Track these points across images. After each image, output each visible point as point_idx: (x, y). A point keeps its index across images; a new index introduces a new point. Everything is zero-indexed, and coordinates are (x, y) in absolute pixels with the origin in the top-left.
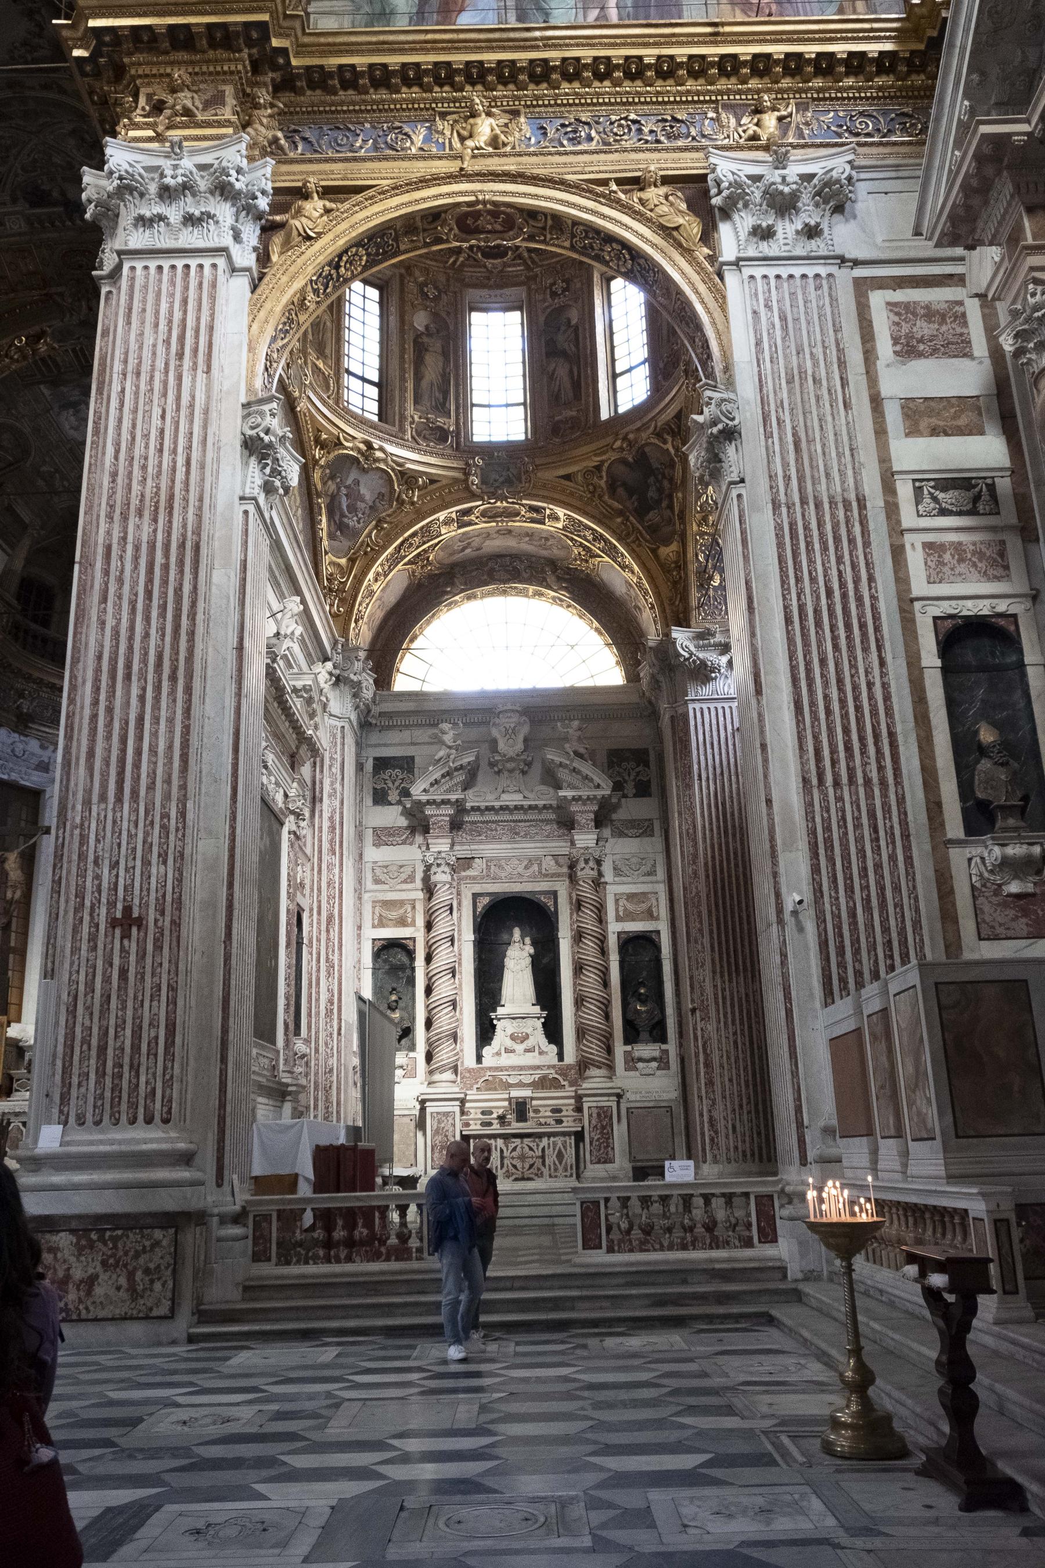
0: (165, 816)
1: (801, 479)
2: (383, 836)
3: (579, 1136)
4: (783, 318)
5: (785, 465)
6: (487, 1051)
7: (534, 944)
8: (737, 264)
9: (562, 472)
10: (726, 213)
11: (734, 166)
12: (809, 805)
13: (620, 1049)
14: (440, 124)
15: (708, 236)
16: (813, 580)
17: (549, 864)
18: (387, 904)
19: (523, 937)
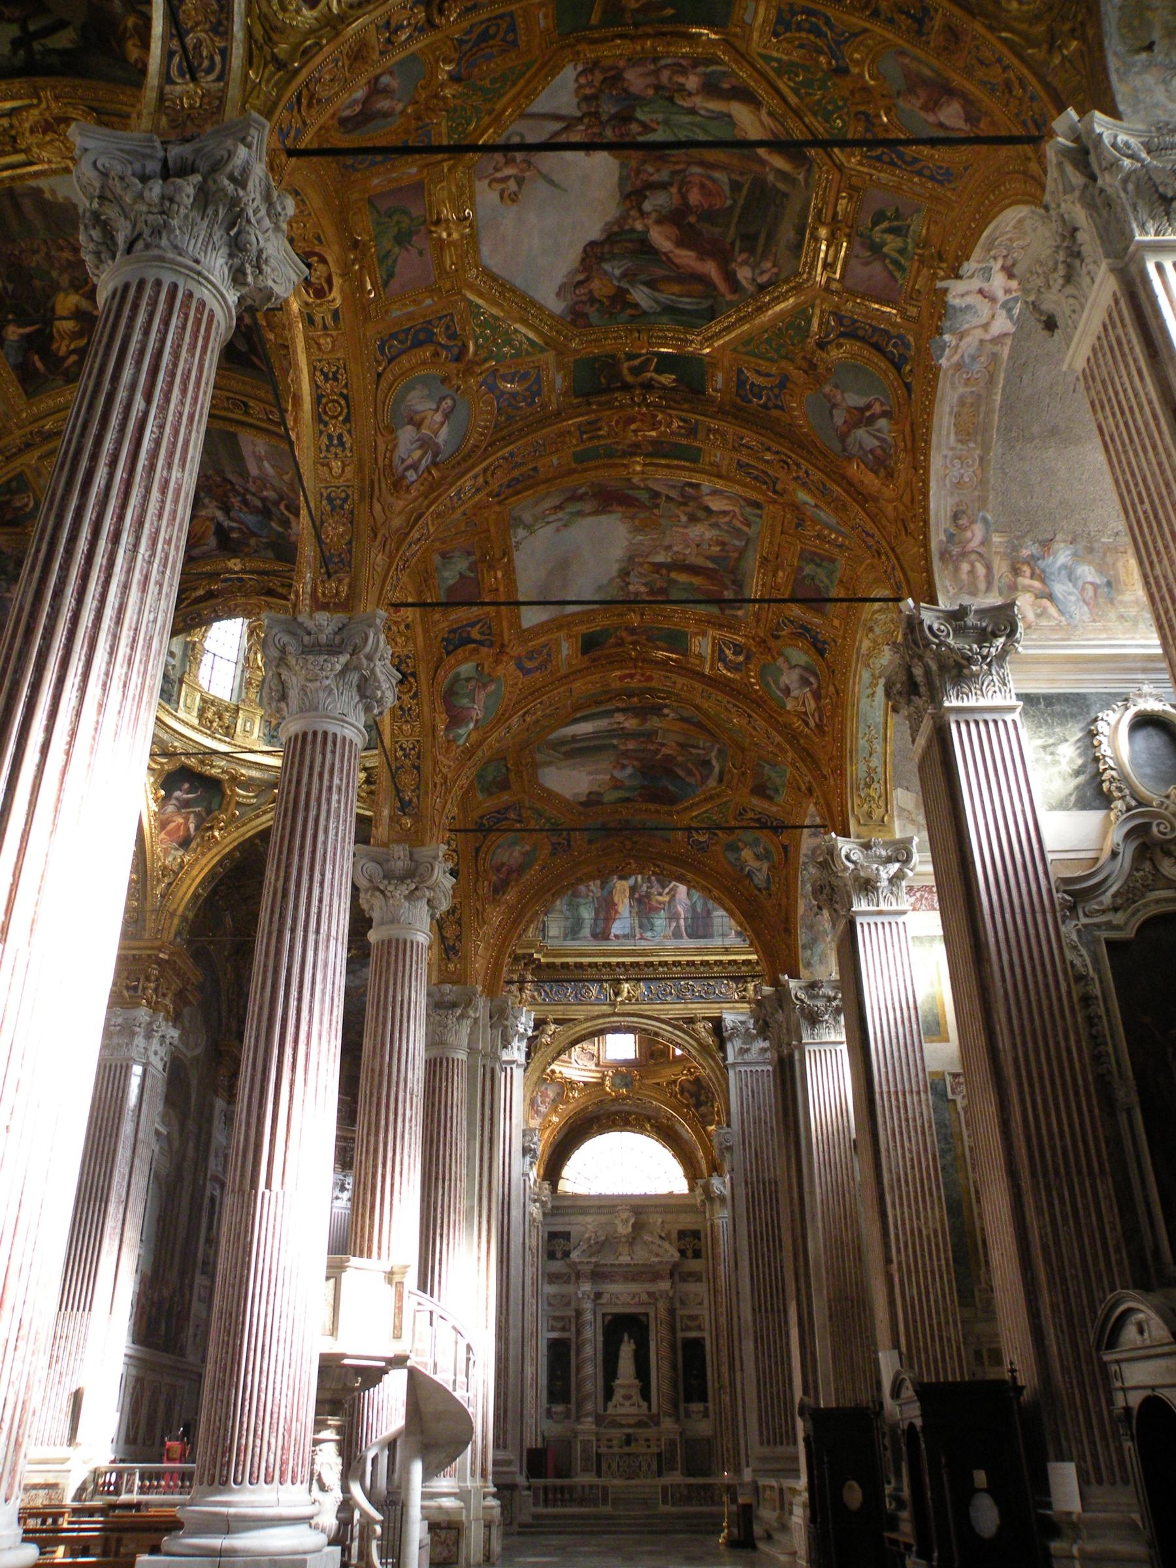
2: (553, 1278)
6: (610, 1404)
8: (734, 1065)
10: (730, 1038)
11: (732, 1017)
12: (755, 1321)
13: (682, 1406)
14: (606, 985)
15: (722, 1048)
17: (644, 1297)
18: (555, 1318)
19: (630, 1337)
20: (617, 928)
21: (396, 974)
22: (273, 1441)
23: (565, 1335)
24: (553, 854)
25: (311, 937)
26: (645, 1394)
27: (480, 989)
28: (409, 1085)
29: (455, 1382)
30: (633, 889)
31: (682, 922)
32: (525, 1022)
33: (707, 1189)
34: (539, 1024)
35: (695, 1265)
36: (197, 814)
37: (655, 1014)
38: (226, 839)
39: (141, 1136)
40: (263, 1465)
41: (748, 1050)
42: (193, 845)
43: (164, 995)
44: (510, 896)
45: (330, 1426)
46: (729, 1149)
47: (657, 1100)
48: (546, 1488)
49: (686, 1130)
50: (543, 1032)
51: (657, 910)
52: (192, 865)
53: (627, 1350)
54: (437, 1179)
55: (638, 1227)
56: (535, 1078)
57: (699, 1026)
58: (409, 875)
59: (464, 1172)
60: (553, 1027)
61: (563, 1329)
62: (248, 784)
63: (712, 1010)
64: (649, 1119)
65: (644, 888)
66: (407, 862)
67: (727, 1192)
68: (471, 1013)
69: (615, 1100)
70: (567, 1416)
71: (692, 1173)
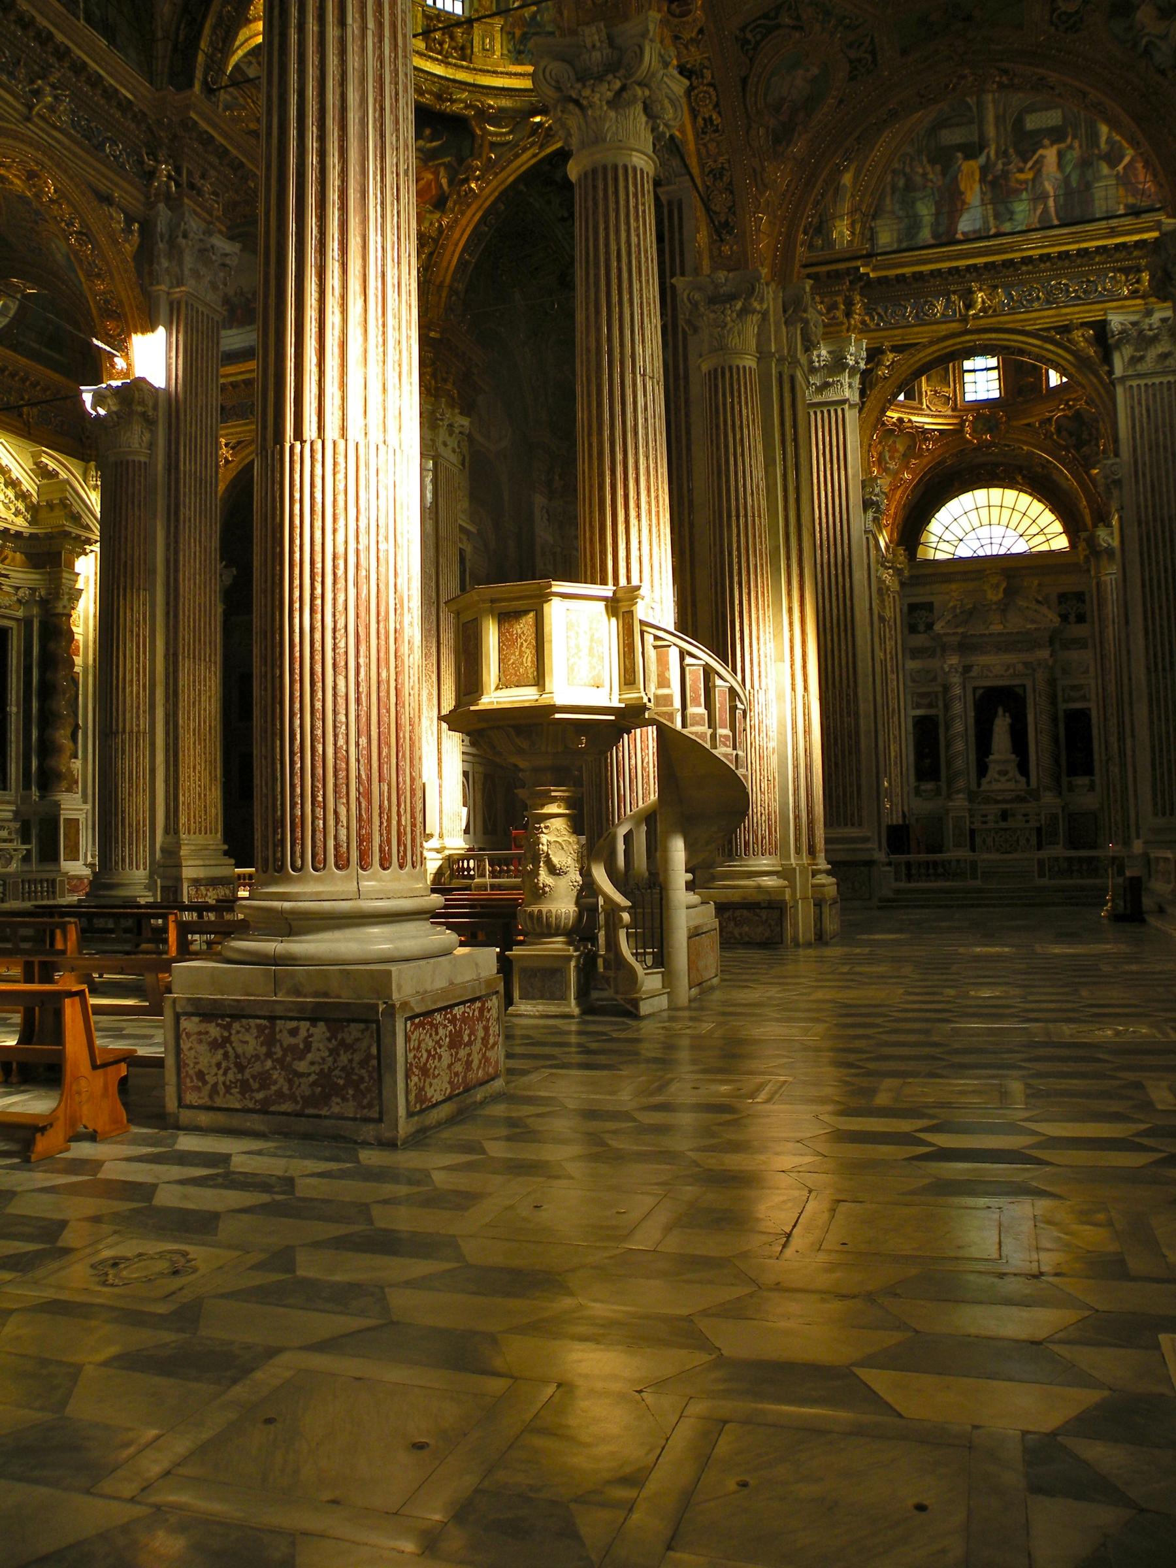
0: (848, 695)
1: (1154, 506)
2: (915, 653)
3: (1039, 830)
4: (1148, 411)
5: (1146, 500)
6: (984, 781)
7: (1011, 717)
8: (1123, 379)
9: (1026, 422)
10: (1117, 346)
11: (1120, 318)
12: (1149, 681)
13: (1065, 780)
14: (954, 298)
15: (1107, 359)
16: (1158, 563)
17: (1020, 667)
18: (922, 695)
19: (1004, 712)
20: (965, 225)
21: (606, 215)
22: (342, 810)
23: (932, 712)
24: (852, 78)
25: (332, 32)
26: (1023, 768)
27: (764, 271)
28: (640, 363)
29: (713, 736)
30: (984, 170)
31: (1051, 203)
32: (855, 353)
33: (1092, 542)
34: (874, 355)
35: (1078, 631)
36: (448, 166)
37: (1018, 326)
38: (482, 189)
39: (442, 533)
40: (331, 843)
41: (1142, 358)
42: (450, 204)
43: (445, 380)
44: (797, 148)
45: (554, 800)
46: (1118, 483)
47: (1026, 443)
48: (908, 865)
49: (1065, 476)
50: (879, 363)
51: (1017, 192)
52: (450, 227)
53: (1001, 726)
54: (729, 516)
55: (1011, 592)
56: (872, 419)
57: (1077, 335)
58: (611, 68)
59: (764, 503)
60: (891, 356)
61: (930, 706)
62: (498, 118)
63: (1092, 314)
64: (1020, 469)
65: (1000, 166)
66: (607, 51)
67: (1116, 543)
68: (756, 305)
69: (978, 448)
70: (938, 792)
71: (1071, 527)
